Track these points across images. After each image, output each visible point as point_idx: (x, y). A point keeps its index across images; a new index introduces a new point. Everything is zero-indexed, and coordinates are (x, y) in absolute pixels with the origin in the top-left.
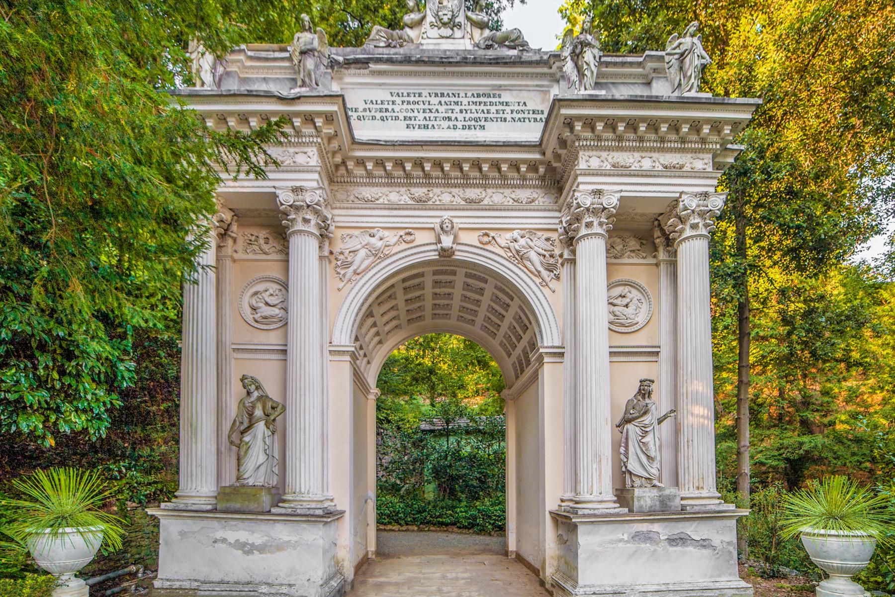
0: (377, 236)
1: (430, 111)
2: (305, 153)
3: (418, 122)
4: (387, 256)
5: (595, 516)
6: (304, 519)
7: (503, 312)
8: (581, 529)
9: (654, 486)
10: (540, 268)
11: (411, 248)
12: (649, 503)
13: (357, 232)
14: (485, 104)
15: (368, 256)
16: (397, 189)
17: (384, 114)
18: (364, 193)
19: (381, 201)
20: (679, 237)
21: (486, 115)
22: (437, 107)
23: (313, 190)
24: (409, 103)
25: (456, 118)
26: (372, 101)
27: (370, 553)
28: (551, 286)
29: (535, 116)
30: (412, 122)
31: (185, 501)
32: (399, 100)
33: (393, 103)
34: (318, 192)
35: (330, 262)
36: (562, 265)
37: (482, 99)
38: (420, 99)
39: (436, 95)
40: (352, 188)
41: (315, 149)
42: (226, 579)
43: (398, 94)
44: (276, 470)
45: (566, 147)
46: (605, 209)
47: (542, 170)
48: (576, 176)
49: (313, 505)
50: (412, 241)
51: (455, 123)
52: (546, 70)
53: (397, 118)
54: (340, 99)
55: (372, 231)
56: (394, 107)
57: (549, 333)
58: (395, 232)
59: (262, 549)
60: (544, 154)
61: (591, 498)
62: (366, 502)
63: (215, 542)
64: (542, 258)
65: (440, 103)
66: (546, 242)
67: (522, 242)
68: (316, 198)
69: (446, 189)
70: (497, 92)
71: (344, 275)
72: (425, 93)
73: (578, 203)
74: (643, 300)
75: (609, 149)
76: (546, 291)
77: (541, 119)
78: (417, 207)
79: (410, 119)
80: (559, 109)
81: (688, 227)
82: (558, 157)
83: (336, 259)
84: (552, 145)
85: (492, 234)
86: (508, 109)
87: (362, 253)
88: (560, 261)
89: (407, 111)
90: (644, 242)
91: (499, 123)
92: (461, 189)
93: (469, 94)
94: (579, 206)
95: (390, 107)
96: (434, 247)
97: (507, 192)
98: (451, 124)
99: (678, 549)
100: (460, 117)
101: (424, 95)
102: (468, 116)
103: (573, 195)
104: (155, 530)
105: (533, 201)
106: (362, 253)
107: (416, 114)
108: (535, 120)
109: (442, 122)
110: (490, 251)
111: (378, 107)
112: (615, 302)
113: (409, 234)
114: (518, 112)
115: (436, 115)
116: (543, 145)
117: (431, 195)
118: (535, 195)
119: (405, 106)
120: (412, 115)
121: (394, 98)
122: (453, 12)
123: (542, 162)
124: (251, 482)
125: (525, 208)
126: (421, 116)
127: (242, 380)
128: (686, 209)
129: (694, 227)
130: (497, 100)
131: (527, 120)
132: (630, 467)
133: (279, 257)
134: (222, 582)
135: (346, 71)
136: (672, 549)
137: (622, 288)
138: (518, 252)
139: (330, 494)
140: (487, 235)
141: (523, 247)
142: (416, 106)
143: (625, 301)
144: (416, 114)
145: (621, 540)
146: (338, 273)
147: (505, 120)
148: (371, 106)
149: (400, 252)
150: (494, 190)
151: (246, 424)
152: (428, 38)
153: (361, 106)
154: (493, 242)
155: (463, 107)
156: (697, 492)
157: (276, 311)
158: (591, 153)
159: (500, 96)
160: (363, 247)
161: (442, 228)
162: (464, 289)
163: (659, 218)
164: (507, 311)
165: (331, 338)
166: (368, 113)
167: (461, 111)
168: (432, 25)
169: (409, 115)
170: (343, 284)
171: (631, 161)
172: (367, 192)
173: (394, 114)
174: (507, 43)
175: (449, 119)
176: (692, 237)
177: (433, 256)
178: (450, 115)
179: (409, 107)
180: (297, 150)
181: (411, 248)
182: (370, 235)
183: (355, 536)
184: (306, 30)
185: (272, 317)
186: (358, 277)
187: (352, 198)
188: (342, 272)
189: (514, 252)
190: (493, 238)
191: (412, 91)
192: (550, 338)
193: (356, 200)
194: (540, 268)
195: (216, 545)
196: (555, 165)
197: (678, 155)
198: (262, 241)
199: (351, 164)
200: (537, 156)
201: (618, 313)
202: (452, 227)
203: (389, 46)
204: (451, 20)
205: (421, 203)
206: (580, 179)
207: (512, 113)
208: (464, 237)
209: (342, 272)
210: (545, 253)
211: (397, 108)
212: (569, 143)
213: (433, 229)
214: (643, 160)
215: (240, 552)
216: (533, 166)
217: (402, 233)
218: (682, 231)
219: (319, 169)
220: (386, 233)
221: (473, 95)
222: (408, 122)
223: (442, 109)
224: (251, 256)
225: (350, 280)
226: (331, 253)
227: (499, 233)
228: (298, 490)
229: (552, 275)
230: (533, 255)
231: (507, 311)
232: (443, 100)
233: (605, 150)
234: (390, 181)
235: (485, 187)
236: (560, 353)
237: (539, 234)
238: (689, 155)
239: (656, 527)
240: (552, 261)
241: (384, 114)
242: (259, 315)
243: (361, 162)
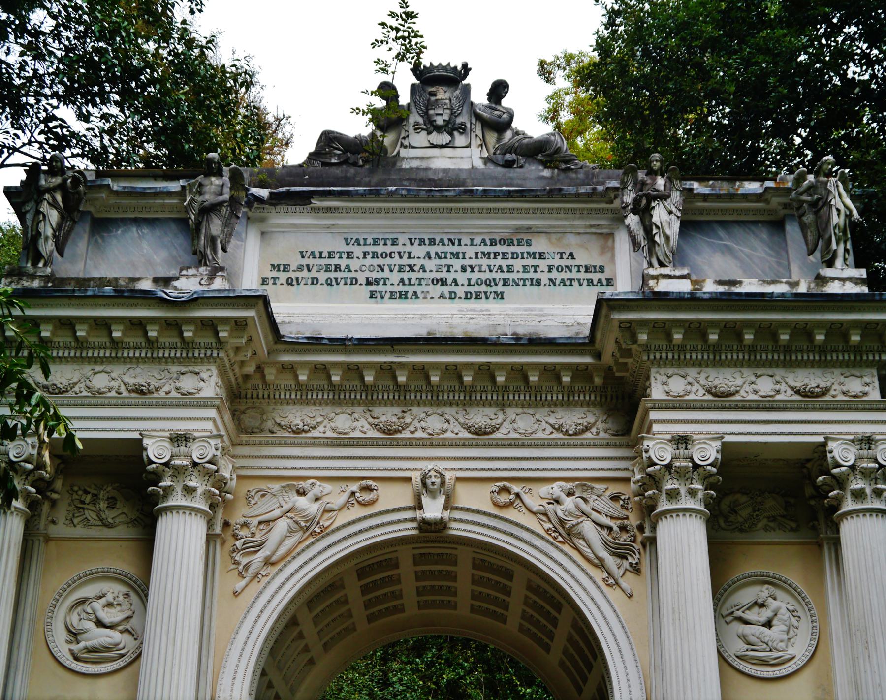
1: (411, 268)
13: (275, 486)
17: (333, 275)
21: (506, 275)
32: (358, 251)
33: (349, 255)
66: (612, 503)
85: (516, 488)
86: (543, 264)
95: (343, 263)
100: (462, 278)
101: (401, 242)
102: (475, 276)
113: (368, 489)
114: (560, 269)
120: (380, 275)
141: (571, 514)
147: (538, 282)
148: (311, 261)
155: (467, 262)
175: (443, 282)
179: (376, 262)
194: (604, 554)
211: (354, 264)
230: (588, 528)
240: (624, 537)
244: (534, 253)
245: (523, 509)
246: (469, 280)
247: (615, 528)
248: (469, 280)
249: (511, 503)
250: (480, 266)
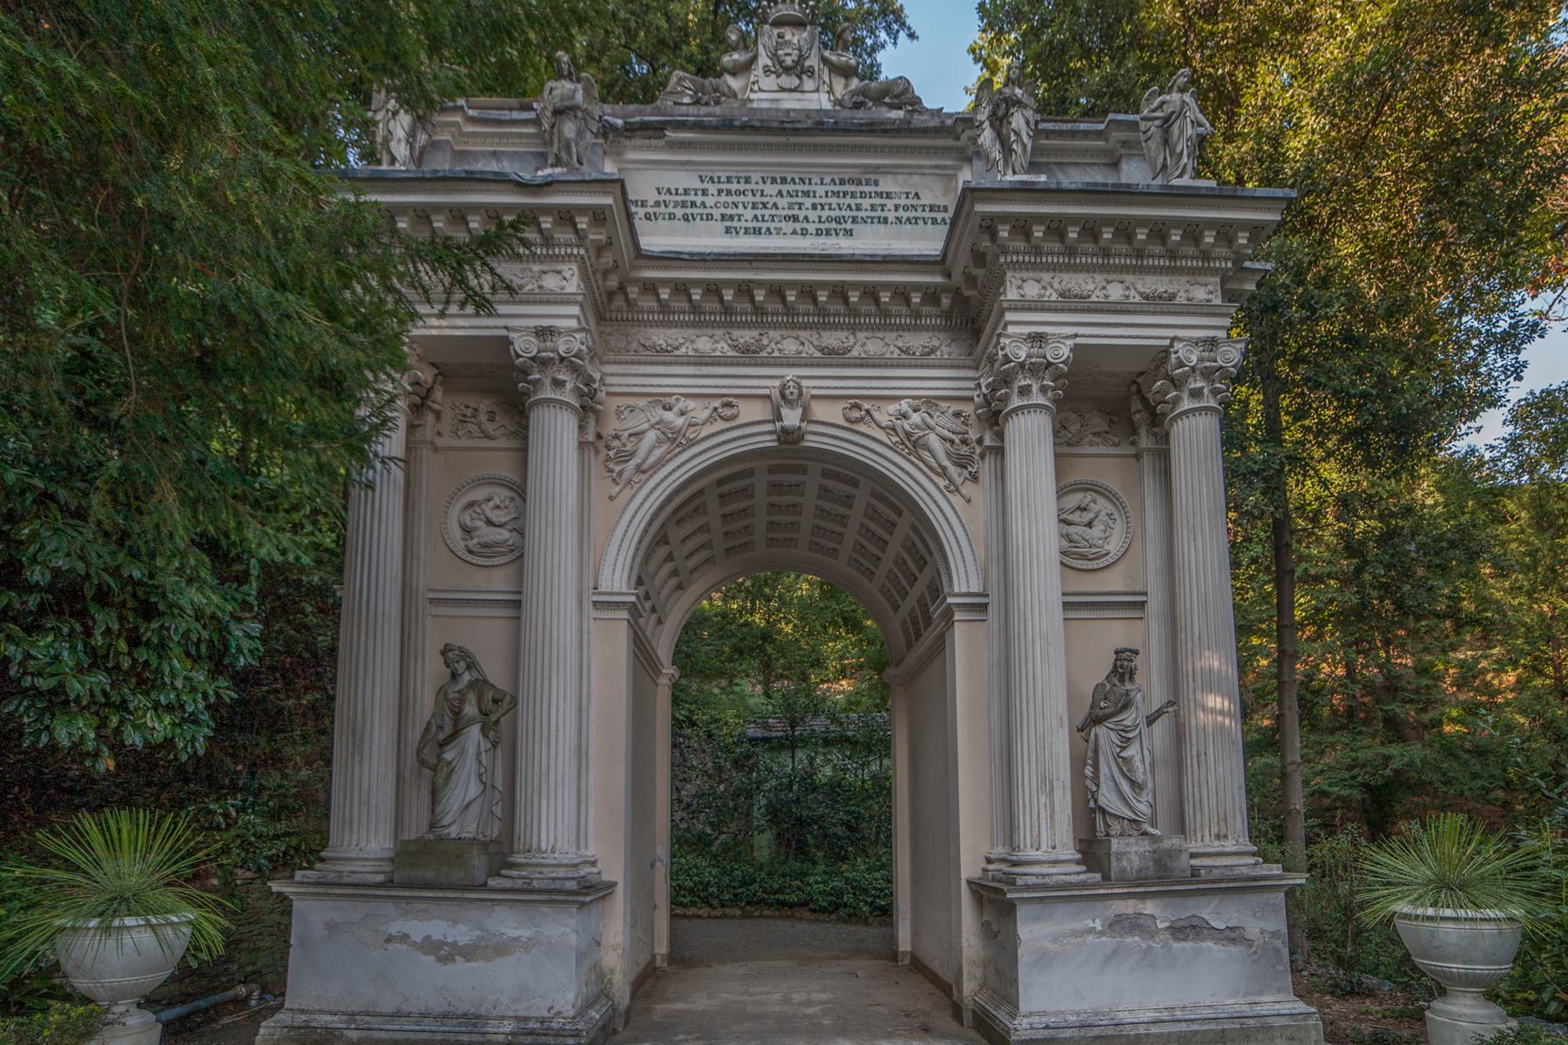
0: (676, 409)
1: (765, 206)
2: (559, 272)
3: (743, 224)
4: (693, 443)
5: (1045, 887)
6: (544, 897)
7: (885, 535)
8: (1022, 912)
9: (1145, 834)
10: (946, 463)
11: (733, 428)
12: (1136, 862)
13: (642, 402)
14: (853, 195)
15: (659, 442)
16: (710, 332)
17: (689, 211)
18: (655, 338)
19: (683, 350)
20: (1173, 409)
21: (855, 213)
23: (570, 332)
24: (729, 192)
25: (806, 218)
26: (669, 191)
27: (659, 958)
28: (964, 491)
29: (933, 215)
30: (735, 224)
31: (338, 868)
32: (712, 189)
33: (705, 192)
34: (578, 336)
35: (597, 452)
36: (982, 456)
37: (848, 188)
38: (748, 187)
39: (774, 181)
40: (635, 330)
41: (574, 267)
42: (405, 1008)
43: (712, 178)
44: (498, 811)
45: (984, 265)
46: (1049, 364)
47: (946, 301)
48: (1002, 313)
49: (561, 873)
50: (734, 417)
51: (805, 225)
52: (950, 142)
53: (710, 217)
54: (618, 186)
55: (668, 400)
56: (705, 199)
57: (962, 570)
58: (706, 402)
59: (470, 952)
60: (949, 275)
61: (1038, 855)
62: (652, 866)
63: (389, 940)
64: (948, 445)
67: (916, 418)
68: (576, 346)
69: (791, 333)
70: (873, 177)
71: (620, 474)
72: (755, 177)
73: (1006, 355)
74: (1116, 516)
75: (1054, 268)
76: (956, 499)
78: (742, 360)
79: (731, 218)
80: (972, 205)
81: (1185, 396)
82: (971, 280)
83: (608, 447)
84: (961, 261)
85: (866, 406)
86: (890, 204)
87: (651, 436)
88: (978, 451)
89: (726, 205)
90: (1115, 419)
91: (876, 226)
92: (814, 333)
93: (827, 180)
94: (1007, 360)
95: (699, 199)
96: (769, 427)
97: (890, 336)
98: (798, 226)
99: (1188, 945)
100: (813, 215)
101: (753, 180)
102: (825, 214)
103: (998, 343)
104: (284, 920)
105: (932, 351)
106: (651, 436)
107: (741, 210)
108: (934, 221)
109: (783, 225)
110: (863, 434)
111: (679, 198)
112: (1071, 518)
113: (729, 405)
114: (906, 208)
115: (774, 212)
116: (948, 262)
117: (765, 342)
118: (936, 343)
119: (723, 198)
120: (734, 212)
121: (705, 185)
122: (800, 50)
123: (945, 289)
124: (454, 831)
125: (919, 362)
126: (749, 214)
127: (443, 653)
128: (1181, 364)
129: (1196, 394)
130: (872, 189)
131: (921, 222)
132: (1102, 801)
133: (512, 443)
134: (397, 1014)
135: (628, 143)
136: (1177, 945)
137: (1080, 495)
138: (908, 435)
139: (591, 852)
140: (858, 407)
141: (917, 427)
142: (742, 198)
144: (741, 210)
145: (1091, 931)
146: (611, 471)
147: (886, 221)
148: (668, 198)
149: (713, 435)
150: (869, 334)
151: (448, 730)
152: (761, 90)
153: (652, 197)
154: (868, 418)
155: (817, 200)
156: (1216, 843)
157: (505, 534)
158: (1025, 275)
159: (876, 183)
160: (652, 427)
161: (783, 396)
162: (819, 497)
163: (1139, 380)
164: (891, 534)
165: (596, 581)
166: (662, 209)
167: (814, 207)
168: (767, 71)
169: (729, 211)
170: (617, 489)
171: (1091, 287)
172: (660, 337)
173: (706, 211)
174: (887, 100)
175: (795, 219)
176: (1193, 411)
177: (769, 442)
178: (796, 212)
179: (730, 199)
180: (545, 268)
181: (733, 428)
182: (664, 408)
183: (633, 927)
184: (564, 77)
185: (498, 544)
186: (644, 477)
187: (635, 345)
188: (617, 469)
189: (902, 435)
190: (868, 412)
191: (734, 174)
192: (964, 579)
193: (641, 349)
194: (946, 463)
195: (389, 946)
196: (967, 293)
197: (1166, 279)
198: (483, 417)
199: (633, 292)
200: (938, 279)
201: (1076, 537)
202: (801, 394)
203: (697, 102)
204: (796, 63)
205: (749, 355)
206: (1009, 316)
207: (896, 210)
208: (821, 411)
209: (617, 469)
210: (954, 437)
211: (710, 201)
212: (989, 258)
213: (768, 397)
214: (1109, 287)
215: (431, 958)
216: (932, 296)
217: (717, 403)
218: (1176, 401)
219: (580, 298)
220: (691, 404)
221: (833, 180)
222: (728, 224)
223: (783, 202)
224: (465, 442)
225: (629, 482)
226: (599, 436)
227: (878, 403)
228: (535, 846)
229: (965, 473)
230: (933, 440)
231: (891, 534)
232: (785, 188)
233: (1048, 270)
234: (698, 319)
235: (853, 328)
236: (980, 605)
237: (944, 405)
238: (1184, 279)
239: (1149, 907)
240: (965, 450)
241: (689, 211)
242: (475, 541)
243: (650, 287)
244: (882, 193)
245: (873, 425)
246: (820, 217)
247: (957, 441)
248: (820, 217)
249: (862, 419)
250: (830, 204)
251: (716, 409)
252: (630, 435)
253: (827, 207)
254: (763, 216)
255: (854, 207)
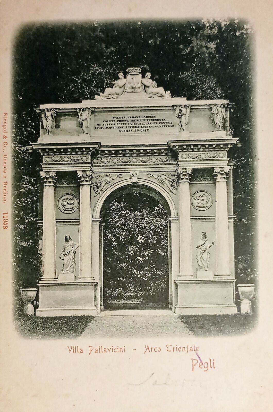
21: (151, 125)
22: (131, 122)
24: (120, 121)
32: (116, 120)
33: (114, 121)
39: (131, 117)
53: (116, 127)
65: (132, 120)
71: (97, 191)
77: (171, 126)
119: (119, 122)
131: (165, 126)
142: (123, 122)
143: (202, 198)
170: (96, 194)
172: (105, 160)
190: (152, 175)
221: (145, 117)
229: (174, 189)
232: (133, 119)
246: (142, 126)
251: (118, 176)
252: (99, 182)
253: (143, 124)
254: (128, 127)
255: (150, 123)
